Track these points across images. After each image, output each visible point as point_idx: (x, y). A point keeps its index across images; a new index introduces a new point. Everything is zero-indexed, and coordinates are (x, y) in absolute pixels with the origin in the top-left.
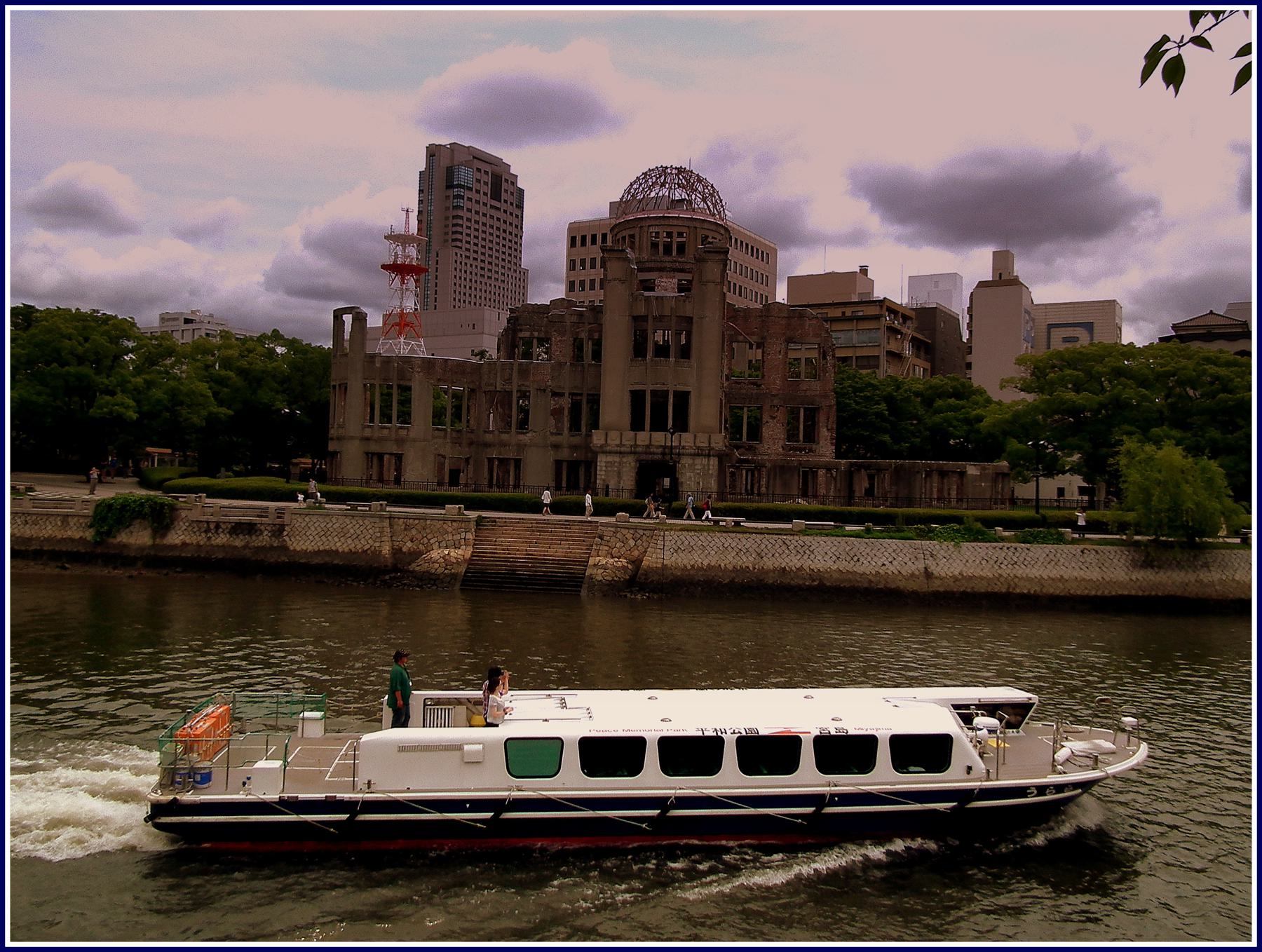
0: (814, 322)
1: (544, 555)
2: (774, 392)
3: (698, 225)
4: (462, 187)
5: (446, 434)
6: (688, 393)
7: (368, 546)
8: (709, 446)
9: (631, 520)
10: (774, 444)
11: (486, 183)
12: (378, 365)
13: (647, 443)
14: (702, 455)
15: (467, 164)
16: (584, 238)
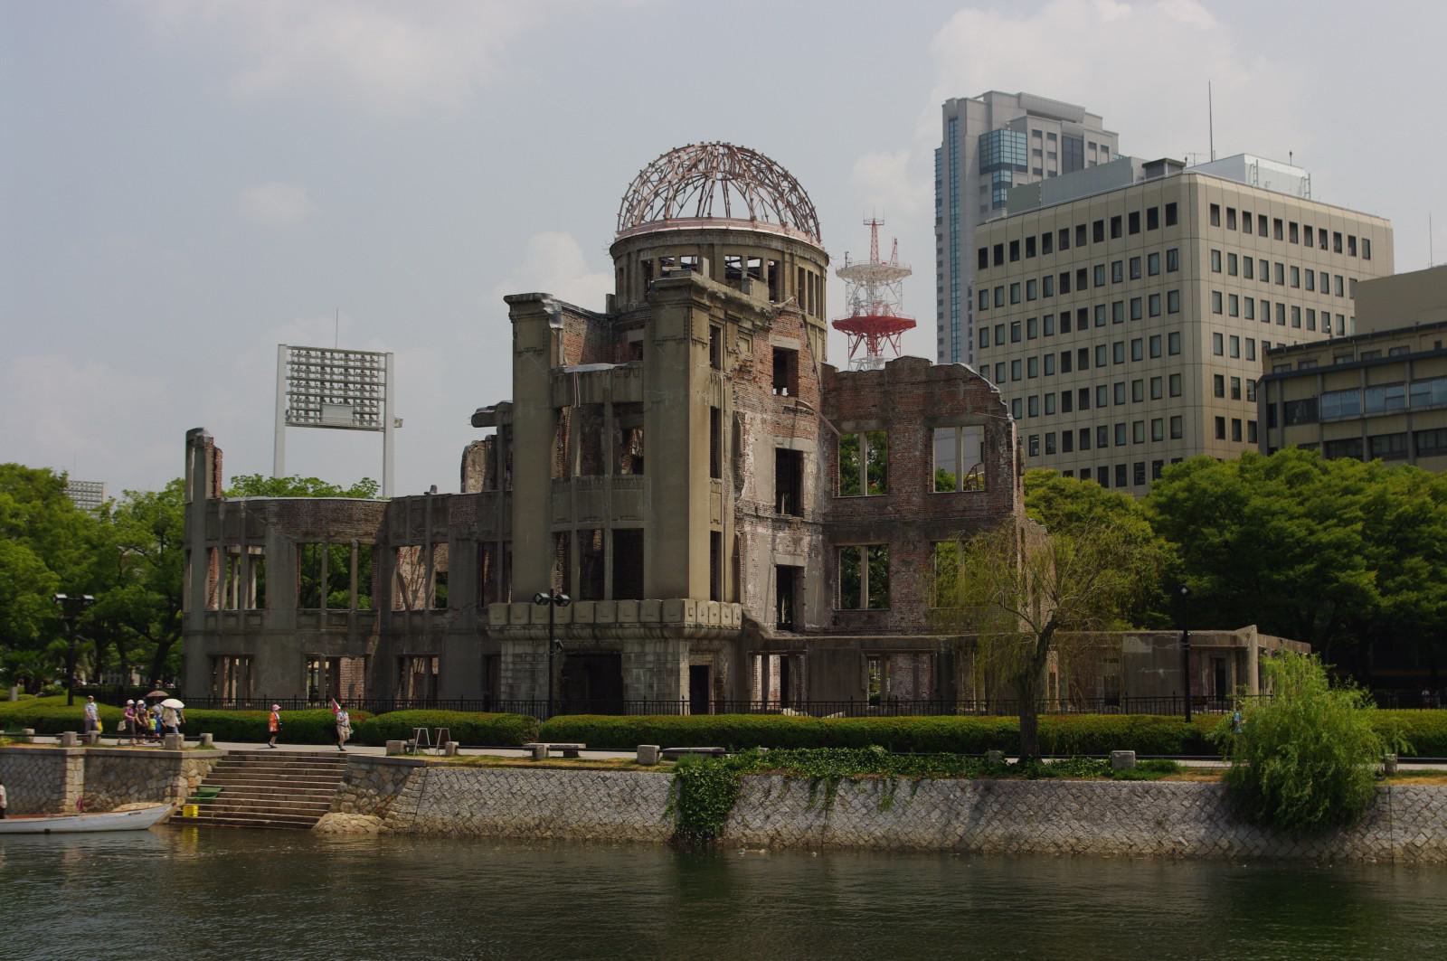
0: (972, 387)
1: (270, 811)
2: (910, 517)
3: (716, 241)
4: (1009, 167)
5: (319, 621)
6: (642, 529)
7: (44, 799)
8: (661, 622)
9: (462, 752)
10: (911, 611)
11: (1053, 155)
12: (222, 517)
13: (567, 620)
14: (654, 638)
15: (1018, 125)
16: (999, 249)
